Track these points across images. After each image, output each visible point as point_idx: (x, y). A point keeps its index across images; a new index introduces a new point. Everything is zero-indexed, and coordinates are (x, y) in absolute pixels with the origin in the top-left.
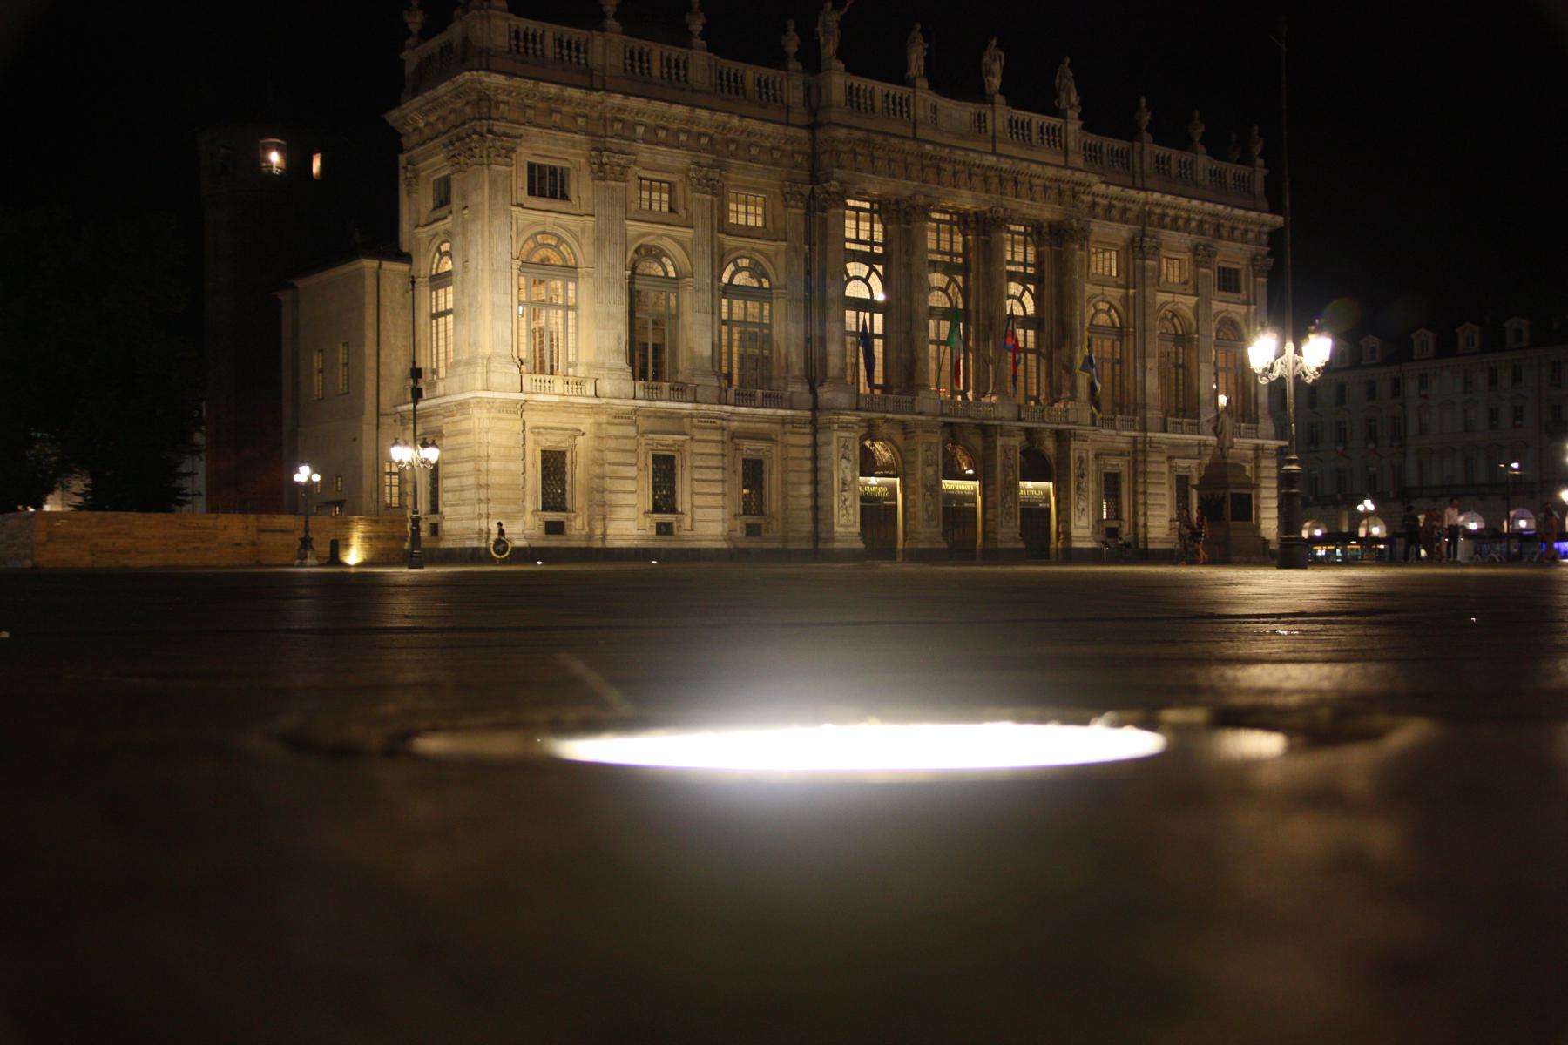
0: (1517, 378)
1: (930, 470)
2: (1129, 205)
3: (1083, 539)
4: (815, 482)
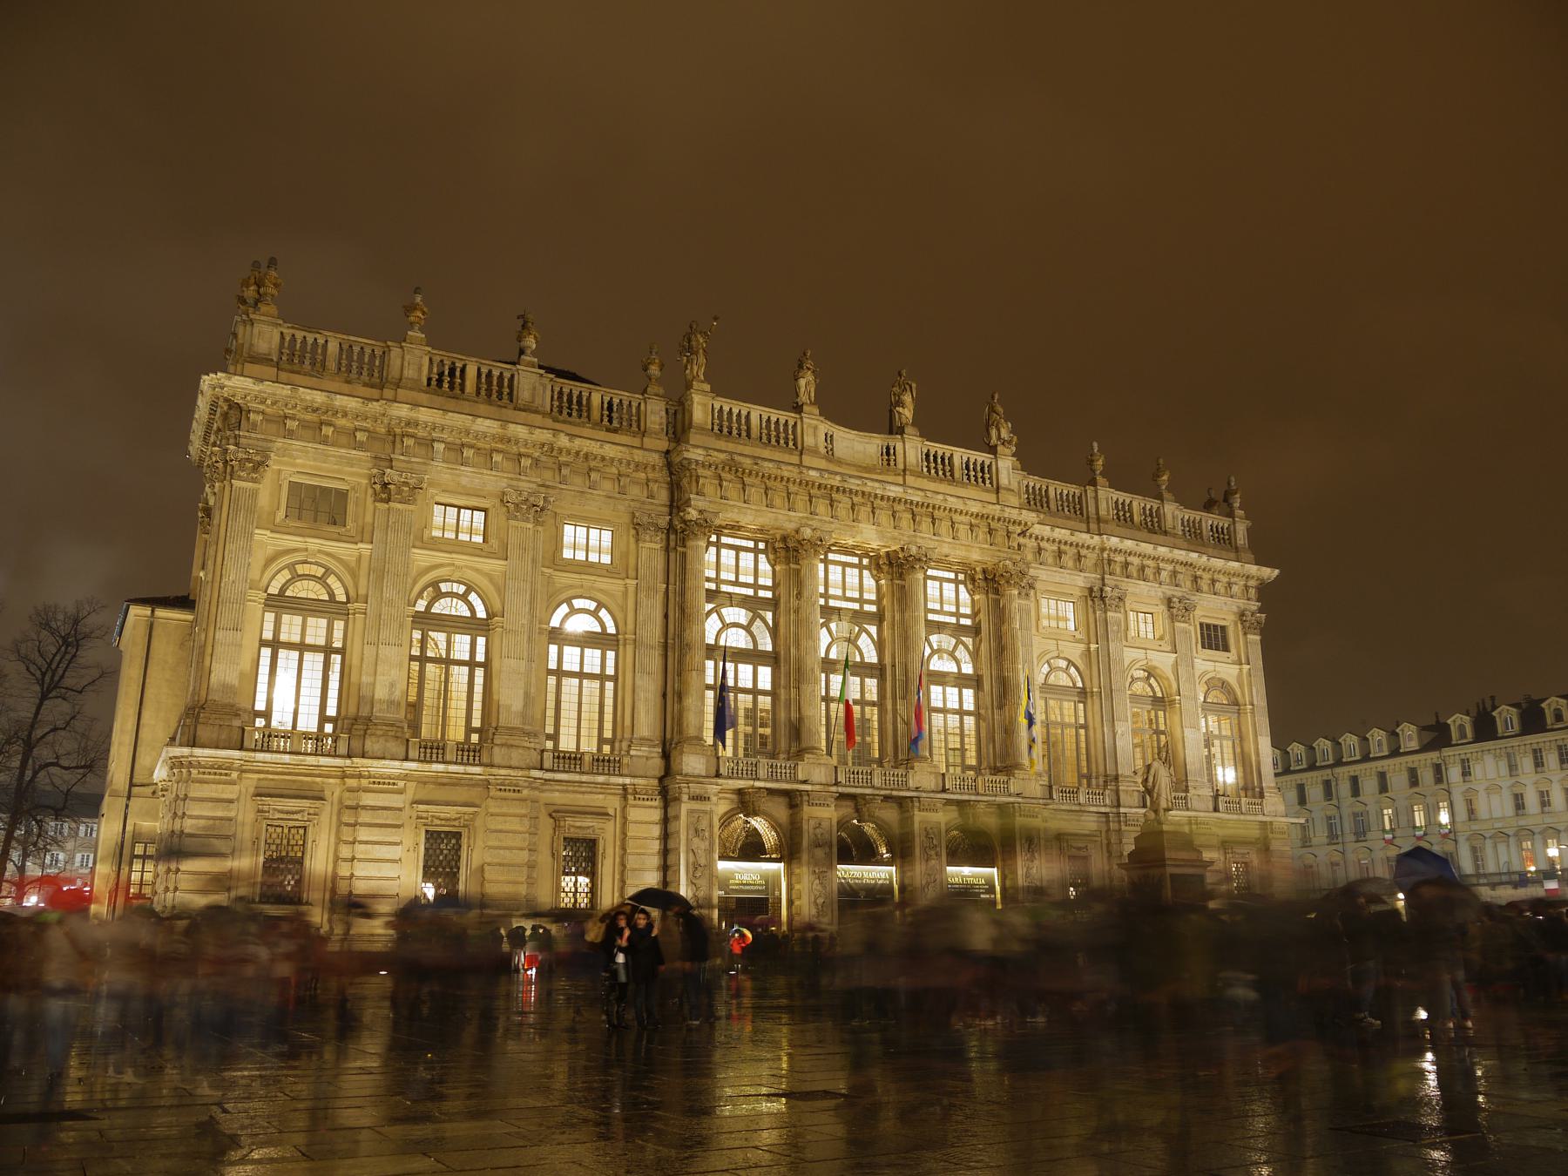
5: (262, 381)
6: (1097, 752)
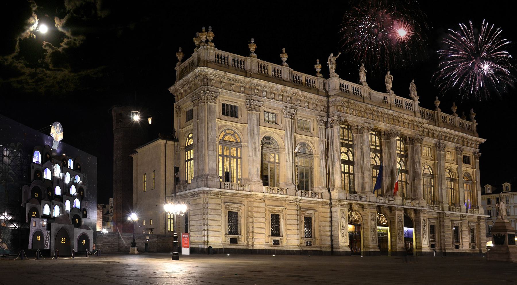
1: (373, 223)
2: (435, 132)
3: (426, 248)
4: (331, 226)
5: (217, 69)
6: (437, 194)
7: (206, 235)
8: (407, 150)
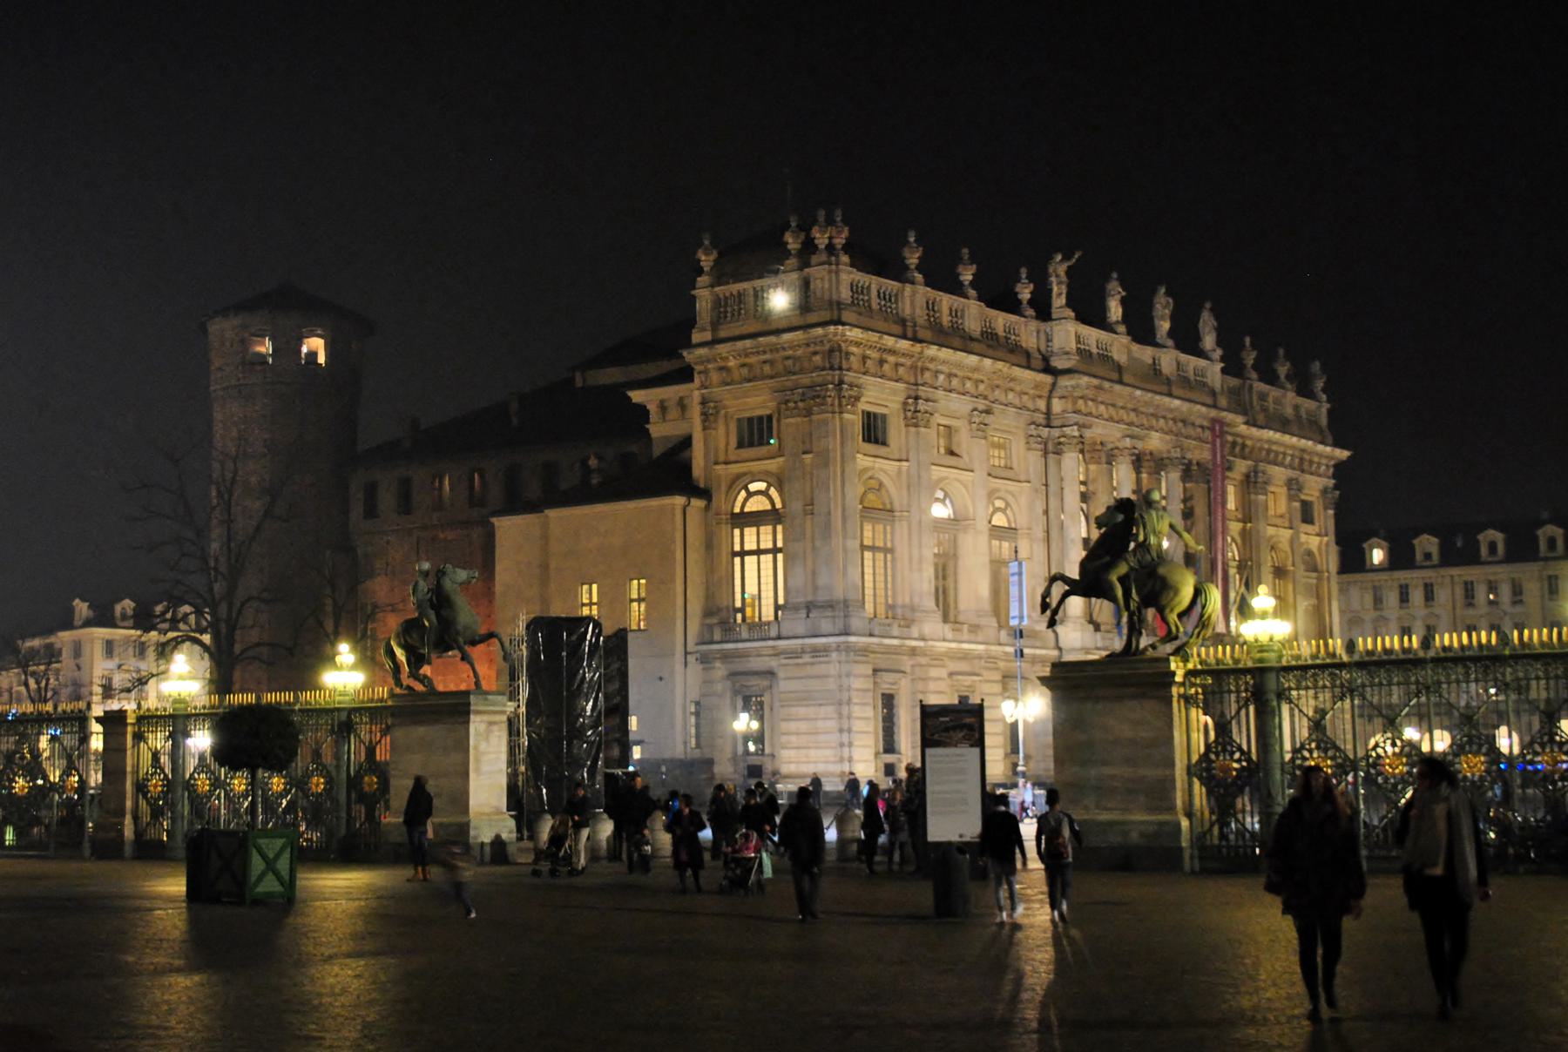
0: (1429, 596)
7: (846, 755)
8: (1191, 498)
